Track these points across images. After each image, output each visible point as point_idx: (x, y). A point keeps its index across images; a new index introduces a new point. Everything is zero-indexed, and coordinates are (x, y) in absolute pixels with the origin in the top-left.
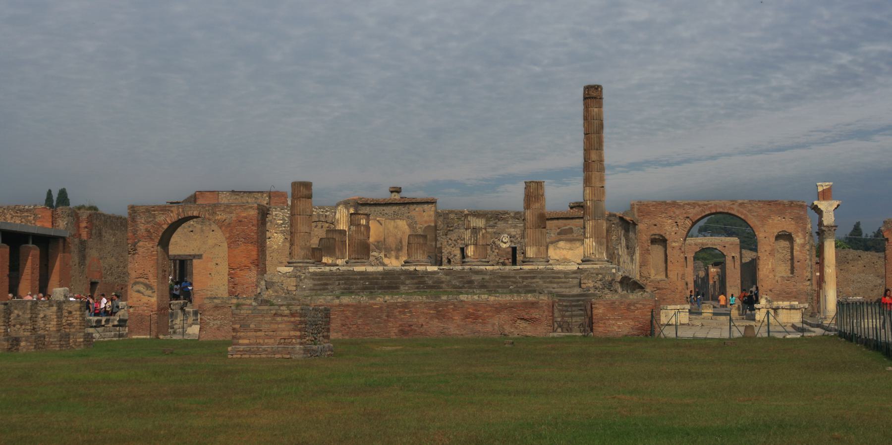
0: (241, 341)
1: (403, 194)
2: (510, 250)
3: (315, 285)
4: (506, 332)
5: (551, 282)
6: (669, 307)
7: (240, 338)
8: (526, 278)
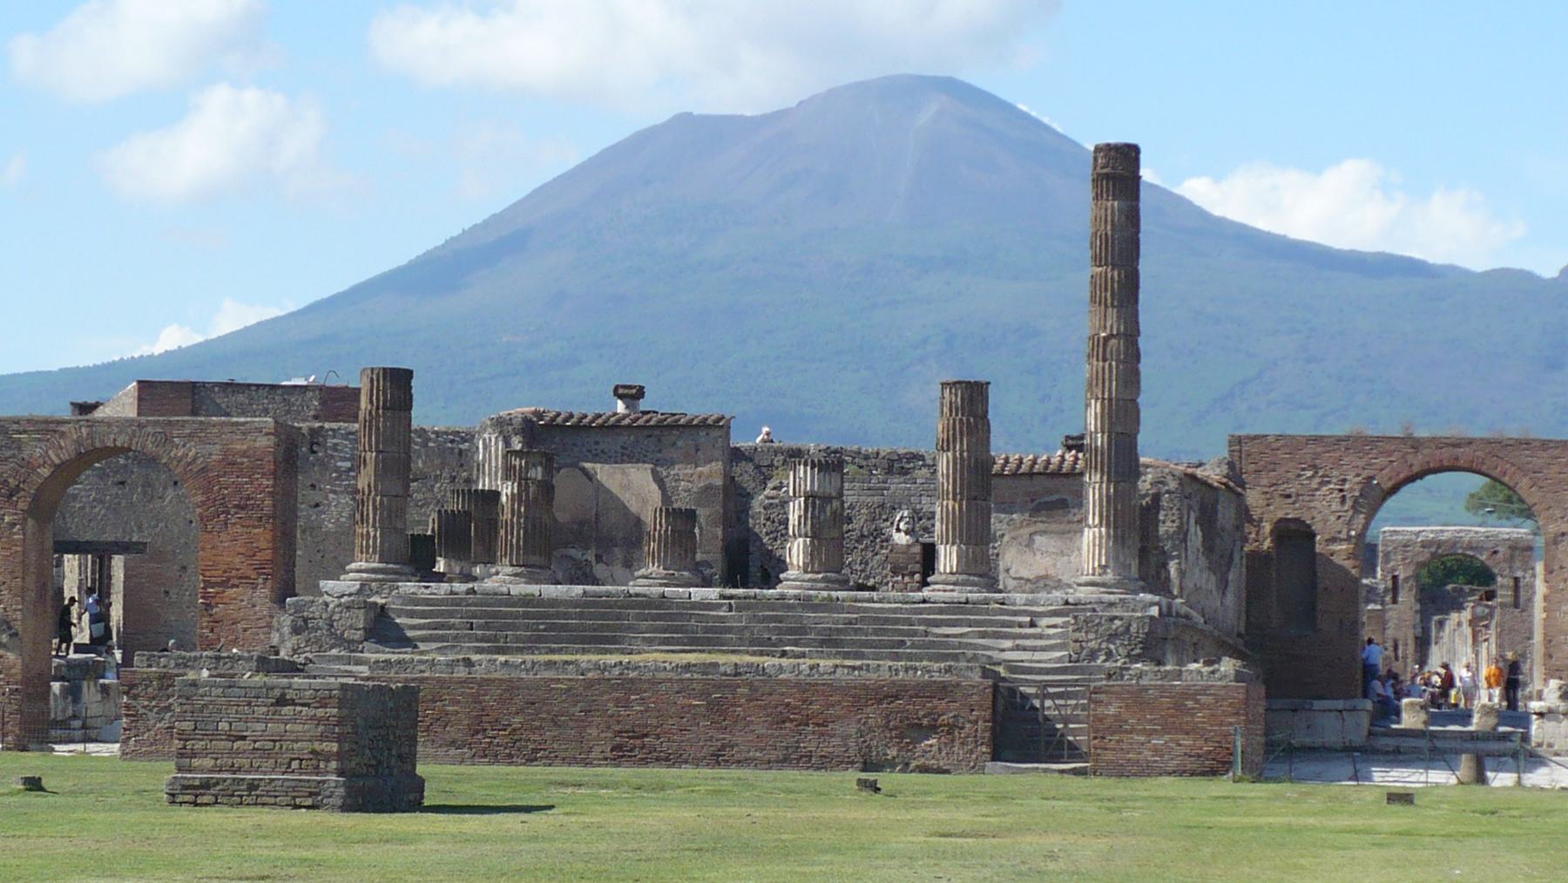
0: (196, 762)
1: (643, 405)
2: (917, 549)
6: (1318, 704)
7: (194, 755)
8: (938, 624)
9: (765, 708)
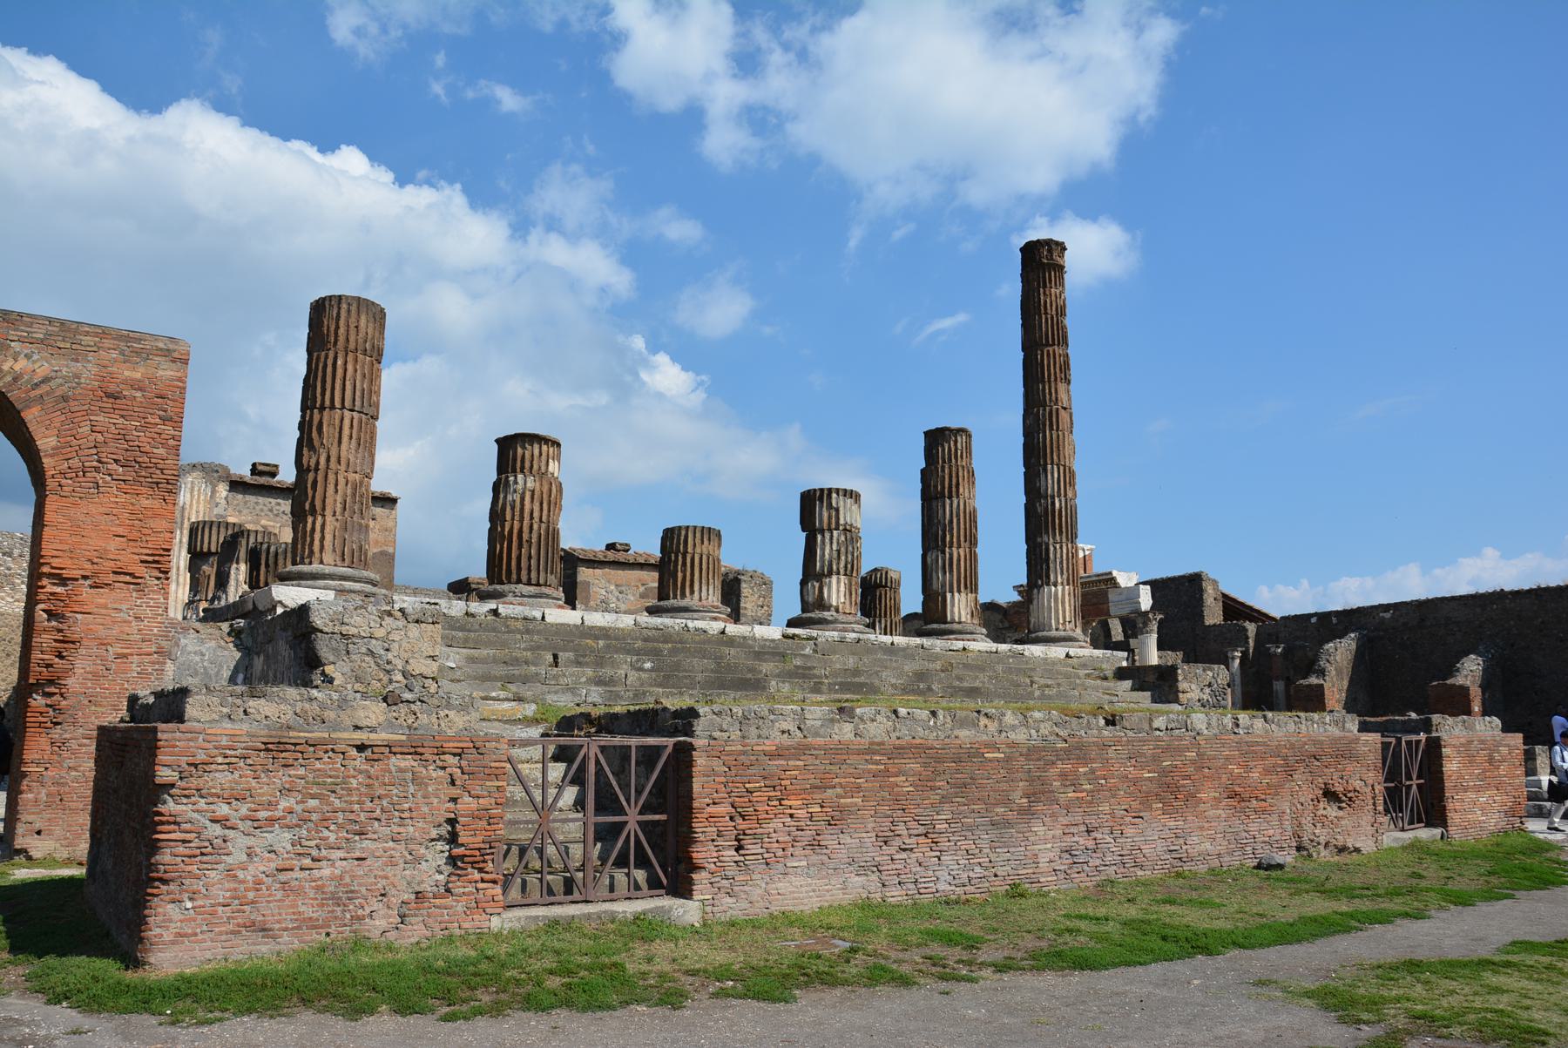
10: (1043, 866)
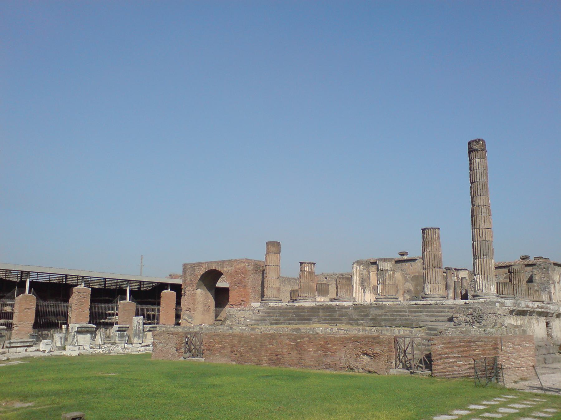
3: (262, 317)
4: (352, 367)
5: (433, 316)
8: (415, 312)
9: (313, 345)
10: (264, 362)
